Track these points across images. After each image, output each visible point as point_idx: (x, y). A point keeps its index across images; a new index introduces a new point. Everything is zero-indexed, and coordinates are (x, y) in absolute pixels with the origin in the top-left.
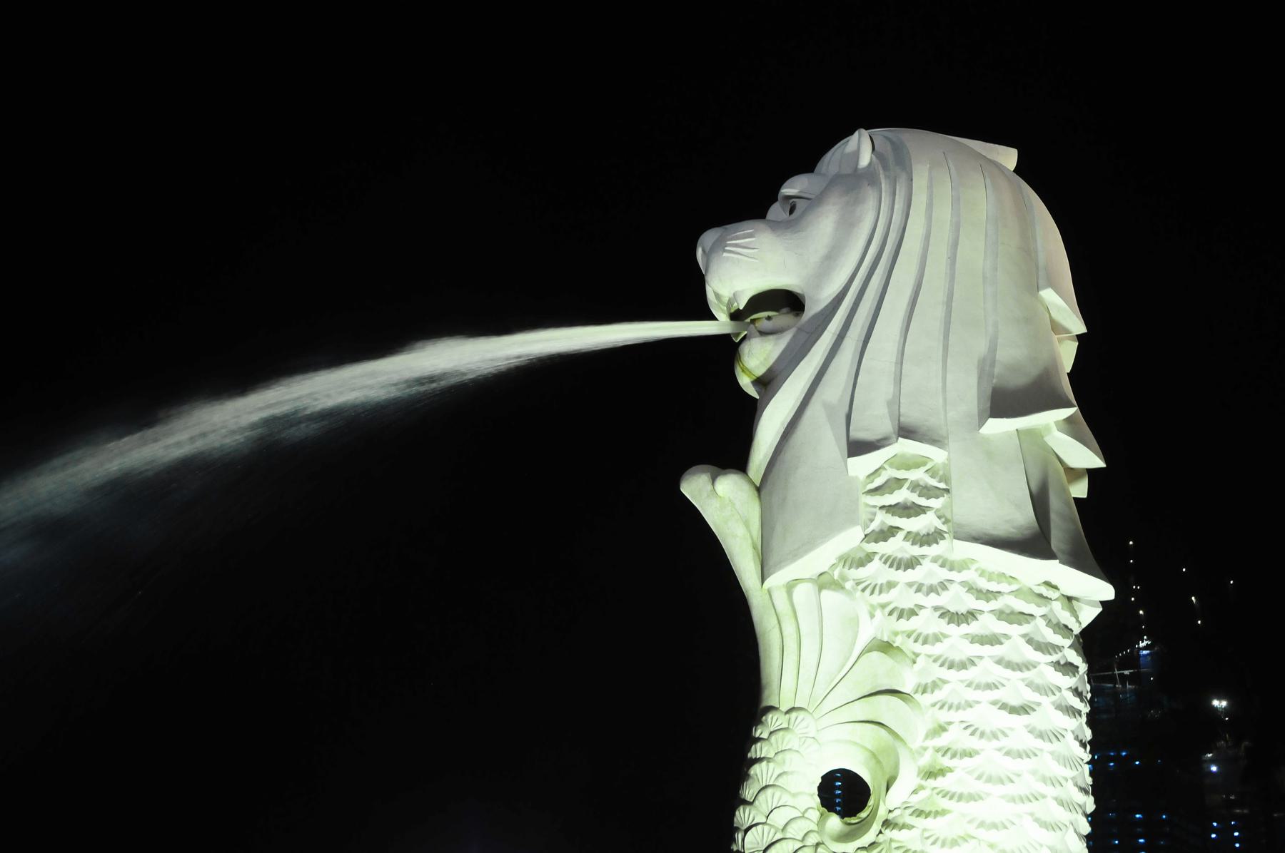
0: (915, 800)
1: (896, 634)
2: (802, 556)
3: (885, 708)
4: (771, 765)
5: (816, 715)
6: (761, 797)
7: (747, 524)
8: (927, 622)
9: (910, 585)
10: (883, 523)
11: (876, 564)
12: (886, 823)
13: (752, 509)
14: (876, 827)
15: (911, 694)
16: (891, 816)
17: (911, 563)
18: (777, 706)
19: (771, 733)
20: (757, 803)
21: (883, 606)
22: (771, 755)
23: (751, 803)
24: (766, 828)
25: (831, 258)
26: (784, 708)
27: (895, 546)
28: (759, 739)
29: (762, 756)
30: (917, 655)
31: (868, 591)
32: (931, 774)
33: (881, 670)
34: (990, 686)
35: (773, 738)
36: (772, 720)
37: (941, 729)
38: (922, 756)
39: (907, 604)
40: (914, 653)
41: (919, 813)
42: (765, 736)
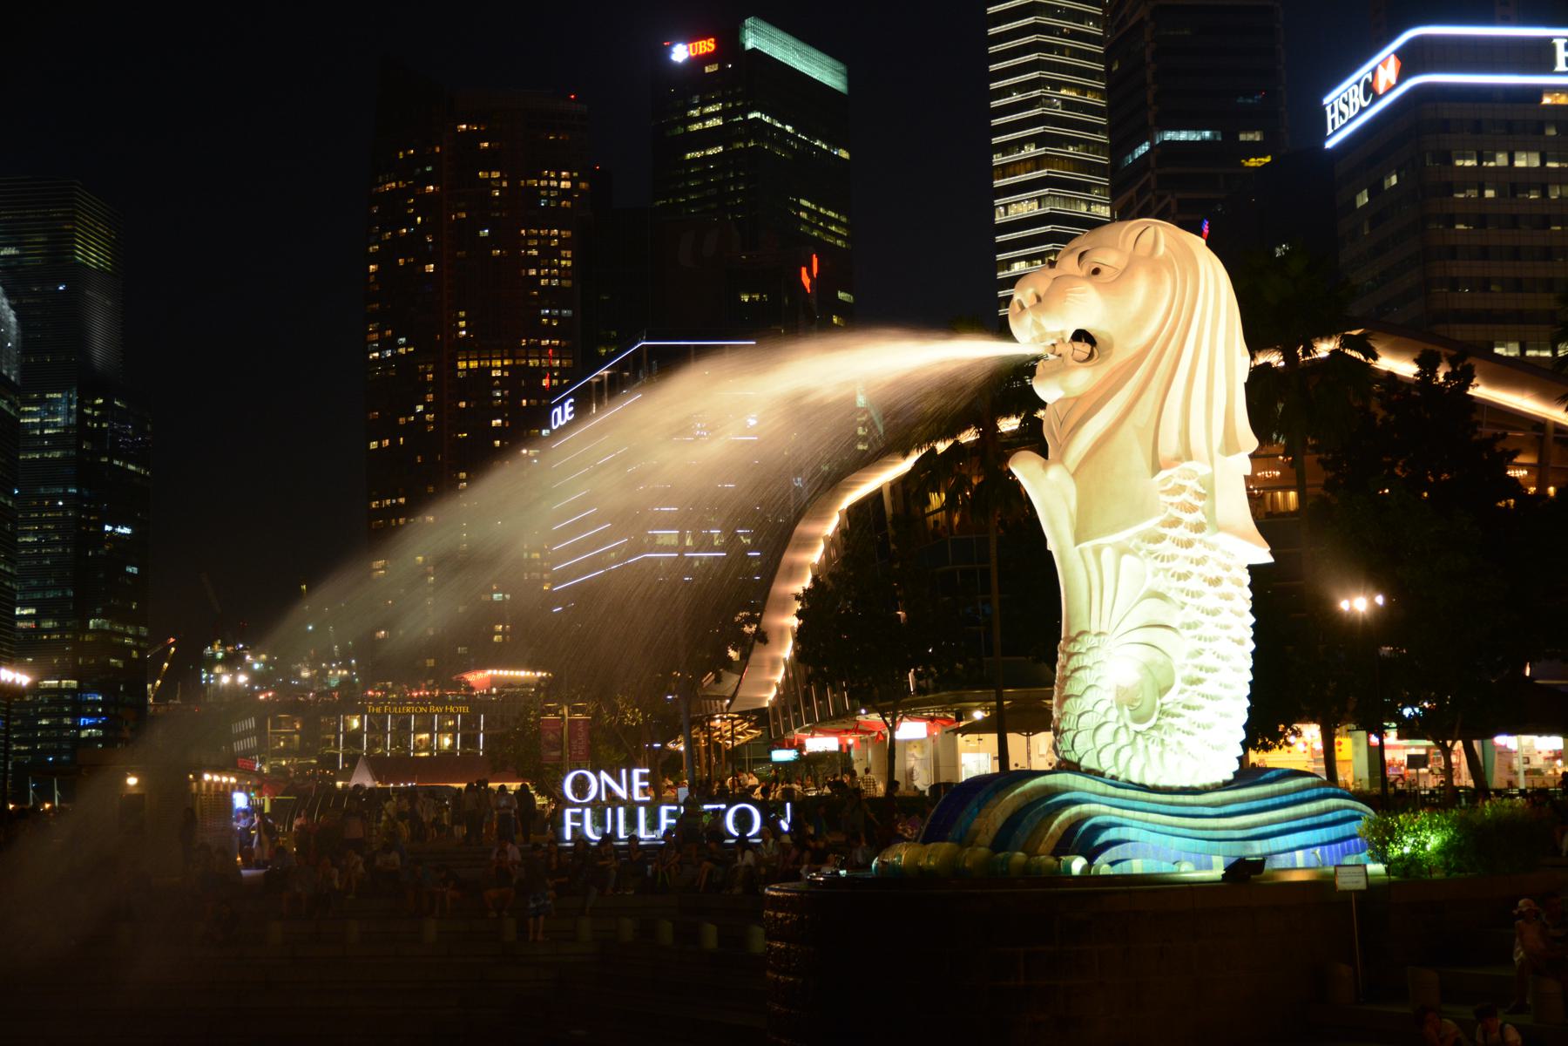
0: (1181, 698)
1: (1170, 589)
2: (1118, 532)
3: (1157, 636)
4: (1093, 671)
6: (1089, 693)
8: (1194, 584)
9: (1186, 558)
10: (1170, 515)
11: (1167, 543)
12: (1162, 712)
13: (1071, 489)
14: (1156, 715)
15: (1178, 628)
16: (1165, 707)
17: (1188, 544)
19: (1088, 649)
20: (1085, 697)
21: (1168, 570)
22: (1090, 664)
24: (1095, 715)
25: (1140, 320)
26: (1094, 631)
27: (1181, 533)
29: (1084, 664)
30: (1185, 604)
31: (1159, 559)
32: (1198, 681)
33: (1154, 610)
34: (1227, 627)
35: (1091, 653)
36: (1088, 641)
37: (1199, 653)
39: (1182, 570)
40: (1182, 602)
42: (1083, 650)
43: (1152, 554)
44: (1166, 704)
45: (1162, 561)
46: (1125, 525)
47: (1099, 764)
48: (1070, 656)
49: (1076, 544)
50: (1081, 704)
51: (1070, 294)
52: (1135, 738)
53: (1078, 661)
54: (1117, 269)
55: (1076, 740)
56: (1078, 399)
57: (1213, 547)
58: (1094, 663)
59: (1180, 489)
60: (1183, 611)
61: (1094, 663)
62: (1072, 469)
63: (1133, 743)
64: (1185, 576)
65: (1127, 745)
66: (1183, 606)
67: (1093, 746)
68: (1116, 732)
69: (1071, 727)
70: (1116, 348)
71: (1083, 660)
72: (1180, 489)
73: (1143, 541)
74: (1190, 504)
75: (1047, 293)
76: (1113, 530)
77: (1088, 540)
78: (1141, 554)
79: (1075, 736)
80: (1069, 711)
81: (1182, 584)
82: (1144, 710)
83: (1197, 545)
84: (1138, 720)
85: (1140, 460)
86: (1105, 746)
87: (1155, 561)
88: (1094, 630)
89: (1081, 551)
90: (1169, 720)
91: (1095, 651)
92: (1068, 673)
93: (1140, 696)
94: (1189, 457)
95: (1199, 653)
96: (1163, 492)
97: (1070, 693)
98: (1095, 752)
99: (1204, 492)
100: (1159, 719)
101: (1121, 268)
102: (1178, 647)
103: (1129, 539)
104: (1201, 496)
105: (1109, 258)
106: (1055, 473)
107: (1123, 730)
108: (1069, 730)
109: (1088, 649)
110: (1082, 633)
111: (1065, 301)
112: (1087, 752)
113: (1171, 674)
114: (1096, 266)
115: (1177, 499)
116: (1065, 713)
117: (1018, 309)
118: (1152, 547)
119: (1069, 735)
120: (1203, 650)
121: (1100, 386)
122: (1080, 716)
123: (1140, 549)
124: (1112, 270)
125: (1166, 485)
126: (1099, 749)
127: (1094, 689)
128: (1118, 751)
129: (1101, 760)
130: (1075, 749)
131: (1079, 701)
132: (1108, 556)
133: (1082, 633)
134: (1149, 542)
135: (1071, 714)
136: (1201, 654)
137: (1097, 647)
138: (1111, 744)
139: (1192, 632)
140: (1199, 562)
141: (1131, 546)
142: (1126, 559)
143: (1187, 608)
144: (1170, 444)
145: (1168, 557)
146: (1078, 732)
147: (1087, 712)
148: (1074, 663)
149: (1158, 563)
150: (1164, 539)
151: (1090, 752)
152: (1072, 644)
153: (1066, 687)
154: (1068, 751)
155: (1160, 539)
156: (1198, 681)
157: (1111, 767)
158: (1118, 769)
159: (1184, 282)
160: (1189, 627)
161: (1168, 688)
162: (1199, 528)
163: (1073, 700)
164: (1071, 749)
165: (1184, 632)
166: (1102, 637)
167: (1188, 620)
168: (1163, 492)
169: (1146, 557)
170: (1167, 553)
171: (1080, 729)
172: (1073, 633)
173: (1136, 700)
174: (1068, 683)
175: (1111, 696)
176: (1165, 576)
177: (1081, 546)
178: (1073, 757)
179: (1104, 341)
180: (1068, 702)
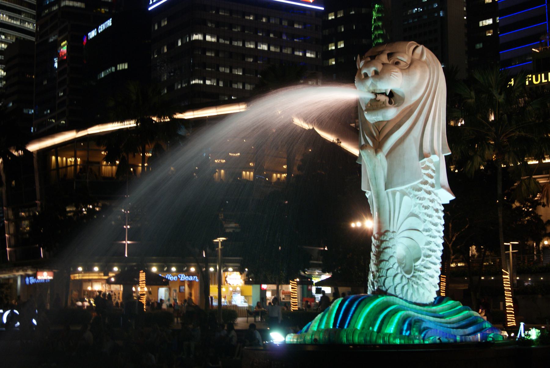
0: (423, 263)
2: (405, 185)
3: (414, 234)
4: (392, 250)
5: (398, 233)
7: (383, 169)
9: (428, 199)
11: (423, 191)
13: (385, 163)
16: (416, 267)
17: (429, 193)
18: (389, 230)
19: (390, 239)
20: (390, 261)
21: (421, 204)
22: (391, 246)
23: (387, 261)
24: (394, 269)
25: (417, 88)
27: (428, 187)
28: (385, 241)
30: (426, 220)
32: (429, 256)
33: (412, 222)
35: (391, 241)
36: (390, 235)
37: (429, 243)
38: (424, 250)
39: (426, 205)
41: (425, 267)
42: (388, 239)
43: (416, 196)
44: (417, 266)
45: (420, 200)
46: (409, 182)
47: (395, 292)
48: (382, 242)
49: (386, 190)
50: (388, 264)
51: (392, 73)
52: (409, 281)
53: (386, 244)
54: (407, 63)
55: (386, 281)
56: (388, 121)
57: (436, 195)
58: (392, 246)
59: (427, 168)
60: (425, 224)
61: (392, 246)
62: (386, 154)
63: (408, 283)
64: (426, 208)
65: (406, 284)
66: (425, 221)
67: (393, 284)
68: (402, 278)
69: (383, 275)
70: (406, 100)
71: (388, 244)
72: (427, 168)
73: (413, 190)
74: (431, 175)
75: (383, 70)
76: (403, 184)
77: (392, 188)
78: (411, 196)
79: (385, 279)
80: (383, 267)
81: (426, 211)
82: (407, 268)
83: (433, 194)
84: (408, 272)
85: (414, 152)
86: (398, 284)
87: (417, 199)
88: (391, 230)
89: (387, 193)
90: (419, 273)
91: (393, 239)
92: (381, 250)
93: (404, 261)
94: (434, 153)
95: (429, 243)
96: (423, 168)
97: (382, 259)
98: (393, 287)
99: (434, 169)
100: (414, 273)
101: (409, 63)
102: (421, 239)
103: (407, 189)
104: (434, 171)
105: (405, 58)
106: (381, 156)
107: (404, 277)
108: (382, 276)
109: (390, 239)
110: (387, 231)
111: (391, 75)
112: (390, 287)
113: (419, 251)
114: (397, 60)
115: (426, 172)
116: (381, 268)
117: (363, 77)
118: (417, 193)
119: (383, 278)
120: (431, 242)
121: (398, 116)
122: (387, 270)
123: (411, 194)
124: (405, 64)
125: (423, 165)
126: (395, 285)
127: (393, 258)
128: (403, 287)
129: (396, 291)
130: (385, 285)
131: (387, 263)
132: (398, 195)
133: (387, 231)
134: (416, 191)
135: (383, 269)
136: (430, 244)
137: (393, 238)
138: (400, 283)
139: (428, 233)
140: (432, 201)
141: (407, 192)
142: (406, 198)
143: (426, 222)
144: (427, 148)
145: (422, 198)
146: (387, 277)
147: (391, 268)
148: (383, 245)
149: (418, 201)
150: (422, 190)
151: (391, 287)
152: (383, 236)
153: (381, 256)
154: (381, 286)
155: (420, 190)
156: (429, 256)
157: (400, 294)
158: (402, 295)
159: (434, 73)
160: (427, 231)
161: (417, 259)
162: (433, 186)
163: (384, 262)
164: (382, 285)
165: (426, 234)
166: (395, 234)
167: (426, 228)
168: (423, 168)
169: (412, 197)
170: (422, 196)
171: (387, 276)
172: (383, 231)
173: (403, 264)
174: (382, 254)
175: (396, 261)
176: (419, 207)
177: (388, 190)
178: (384, 289)
179: (399, 96)
180: (382, 263)
